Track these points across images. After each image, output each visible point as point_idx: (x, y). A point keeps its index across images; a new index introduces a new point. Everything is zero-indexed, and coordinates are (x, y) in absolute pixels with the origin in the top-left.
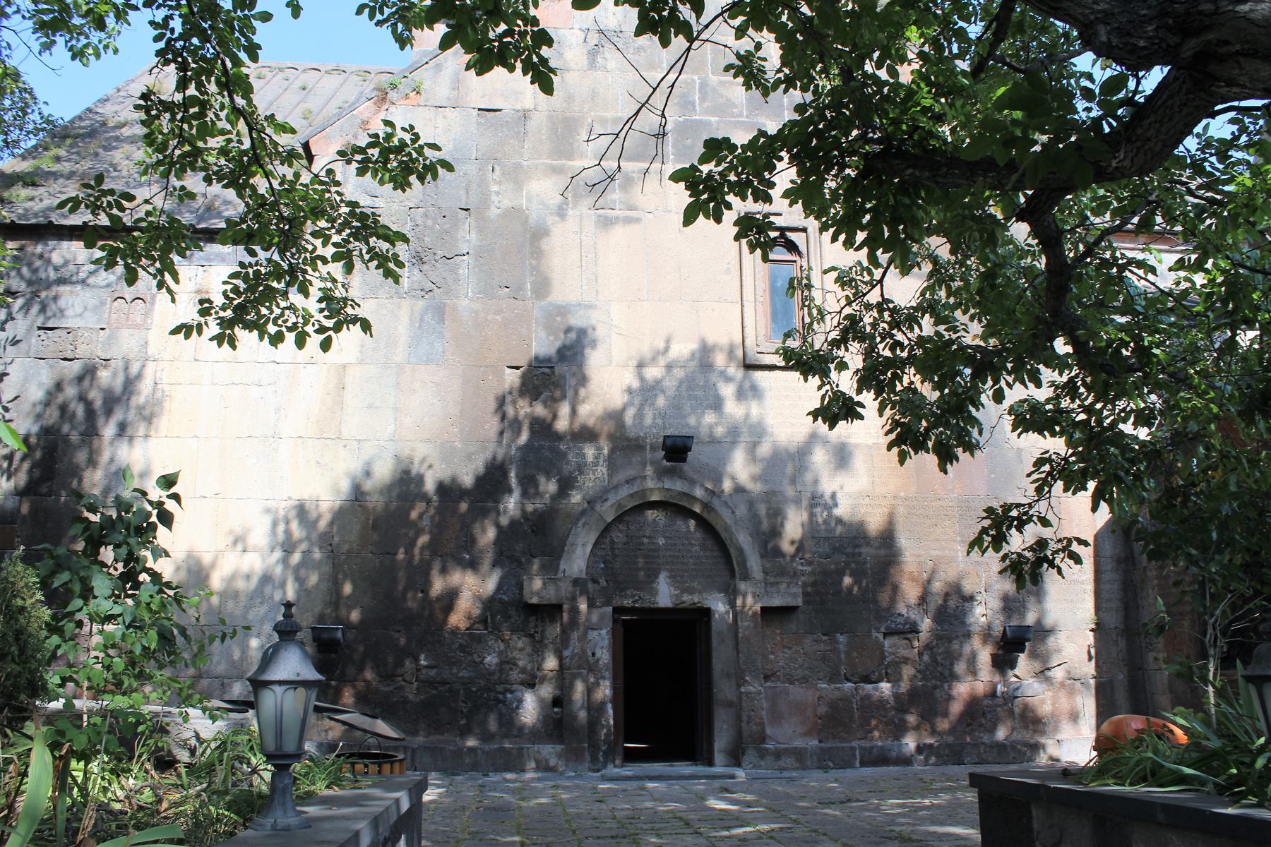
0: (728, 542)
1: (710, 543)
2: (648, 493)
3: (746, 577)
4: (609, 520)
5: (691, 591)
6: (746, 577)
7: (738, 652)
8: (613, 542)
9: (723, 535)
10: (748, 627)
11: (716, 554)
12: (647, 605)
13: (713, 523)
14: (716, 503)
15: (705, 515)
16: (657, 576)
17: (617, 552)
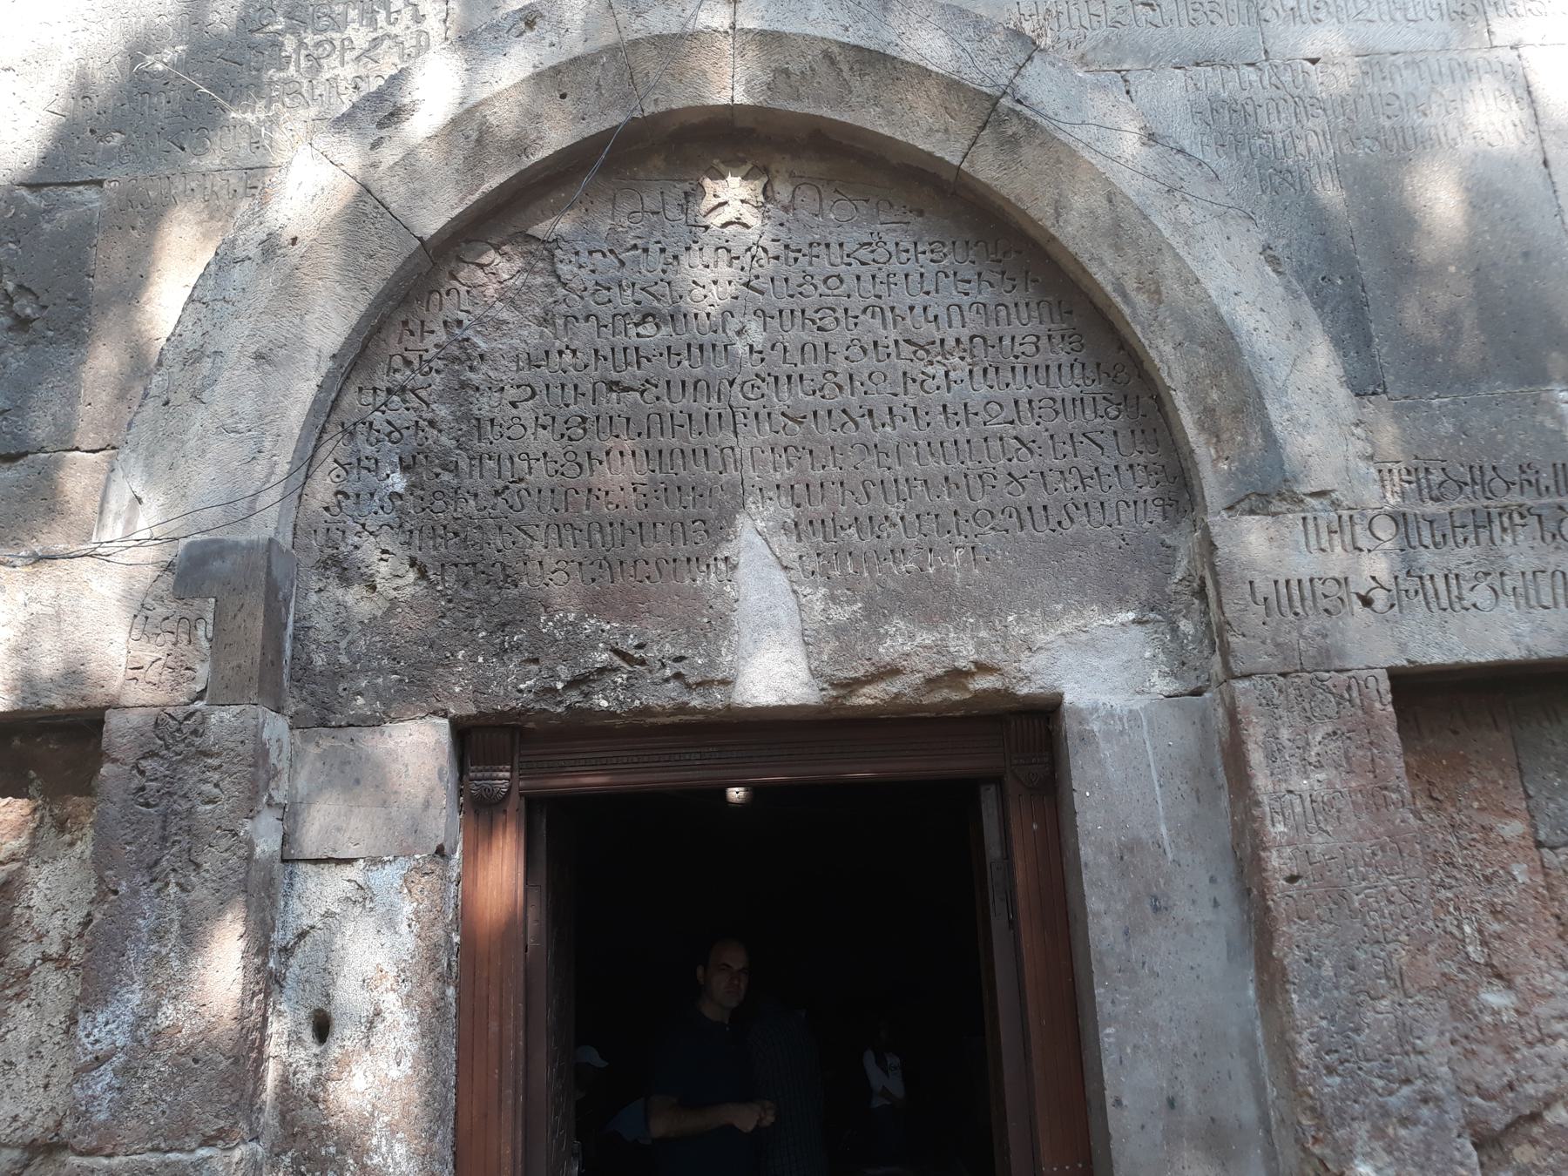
0: (1136, 312)
1: (1025, 326)
2: (649, 65)
3: (1269, 491)
4: (433, 220)
5: (932, 602)
6: (1269, 491)
7: (1272, 981)
8: (462, 356)
9: (1106, 270)
10: (1321, 808)
11: (1066, 388)
12: (660, 696)
13: (1039, 210)
14: (1043, 87)
15: (987, 169)
16: (718, 527)
17: (485, 405)
